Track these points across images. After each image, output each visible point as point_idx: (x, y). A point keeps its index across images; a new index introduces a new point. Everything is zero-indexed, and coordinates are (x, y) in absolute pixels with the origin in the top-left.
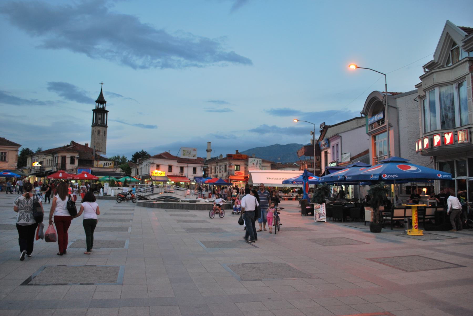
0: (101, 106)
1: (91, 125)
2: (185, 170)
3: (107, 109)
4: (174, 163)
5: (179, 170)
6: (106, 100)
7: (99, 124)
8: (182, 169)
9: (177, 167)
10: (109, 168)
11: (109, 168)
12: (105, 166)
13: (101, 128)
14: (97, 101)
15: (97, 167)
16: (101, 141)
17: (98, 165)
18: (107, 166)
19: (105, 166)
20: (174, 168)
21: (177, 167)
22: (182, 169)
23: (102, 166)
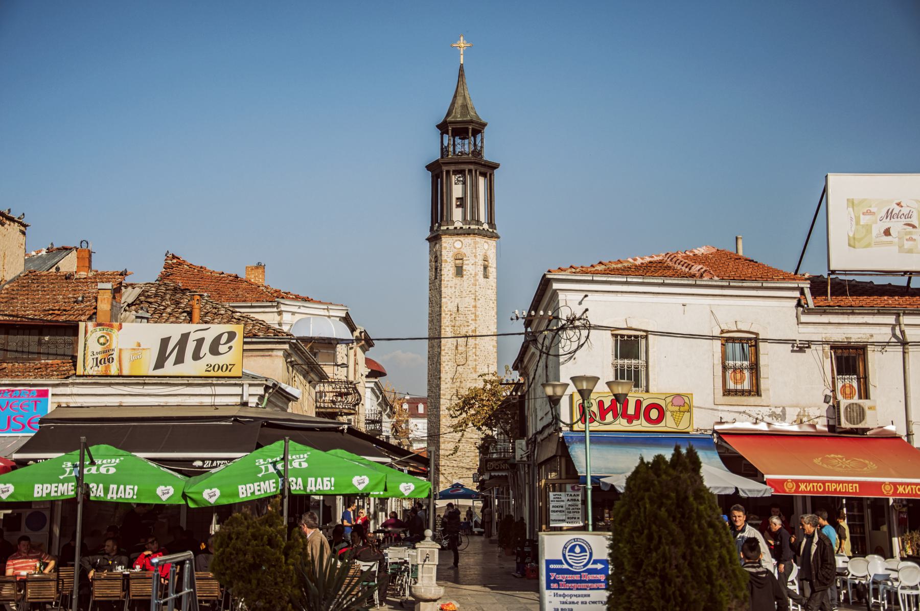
0: (464, 146)
1: (428, 234)
2: (882, 366)
3: (487, 156)
4: (769, 314)
5: (817, 368)
6: (484, 120)
7: (458, 225)
8: (849, 360)
9: (802, 347)
10: (205, 380)
11: (205, 380)
12: (170, 368)
13: (468, 240)
14: (443, 127)
15: (105, 379)
16: (469, 301)
17: (107, 357)
18: (189, 367)
19: (170, 368)
20: (769, 355)
21: (802, 347)
22: (849, 360)
23: (147, 367)
